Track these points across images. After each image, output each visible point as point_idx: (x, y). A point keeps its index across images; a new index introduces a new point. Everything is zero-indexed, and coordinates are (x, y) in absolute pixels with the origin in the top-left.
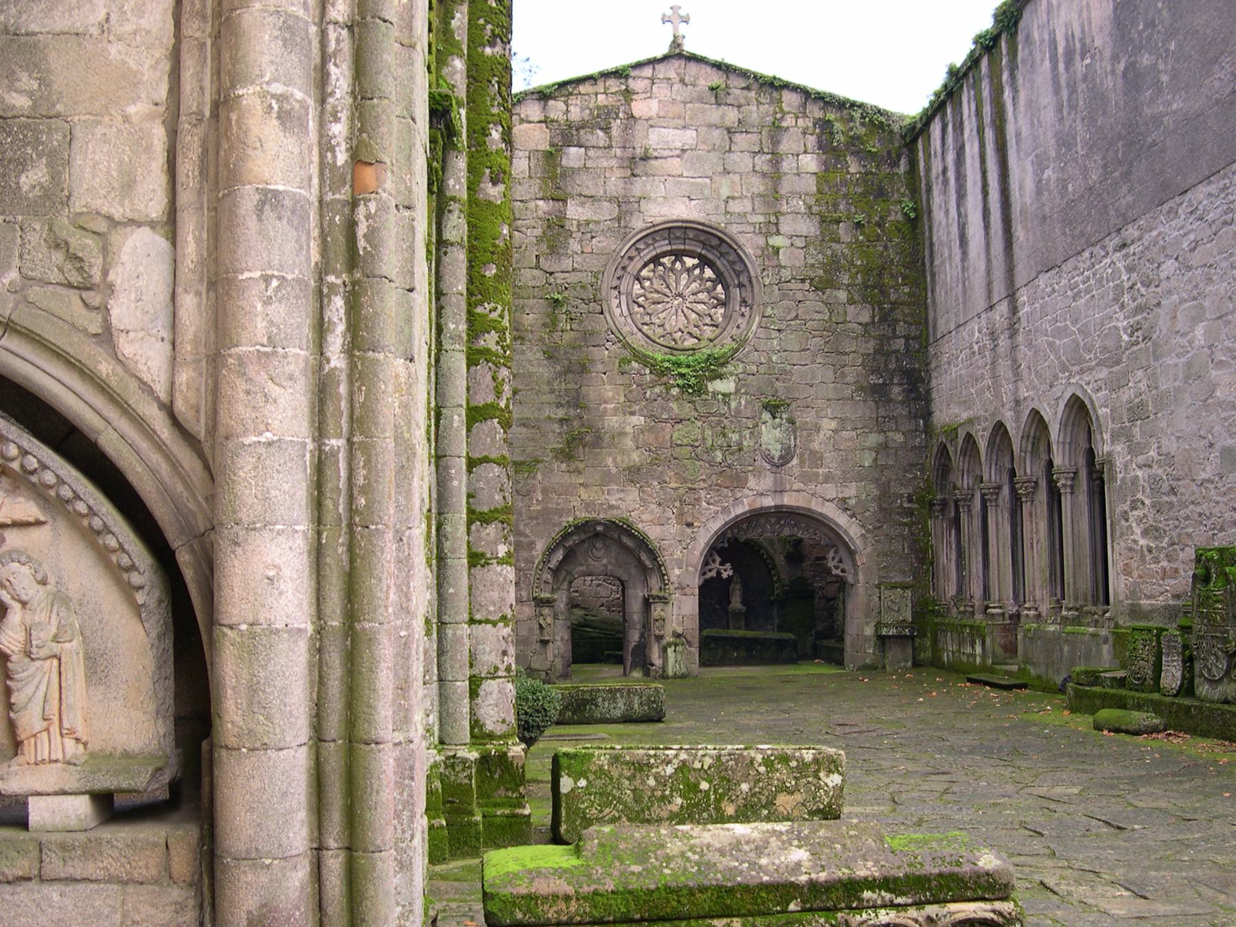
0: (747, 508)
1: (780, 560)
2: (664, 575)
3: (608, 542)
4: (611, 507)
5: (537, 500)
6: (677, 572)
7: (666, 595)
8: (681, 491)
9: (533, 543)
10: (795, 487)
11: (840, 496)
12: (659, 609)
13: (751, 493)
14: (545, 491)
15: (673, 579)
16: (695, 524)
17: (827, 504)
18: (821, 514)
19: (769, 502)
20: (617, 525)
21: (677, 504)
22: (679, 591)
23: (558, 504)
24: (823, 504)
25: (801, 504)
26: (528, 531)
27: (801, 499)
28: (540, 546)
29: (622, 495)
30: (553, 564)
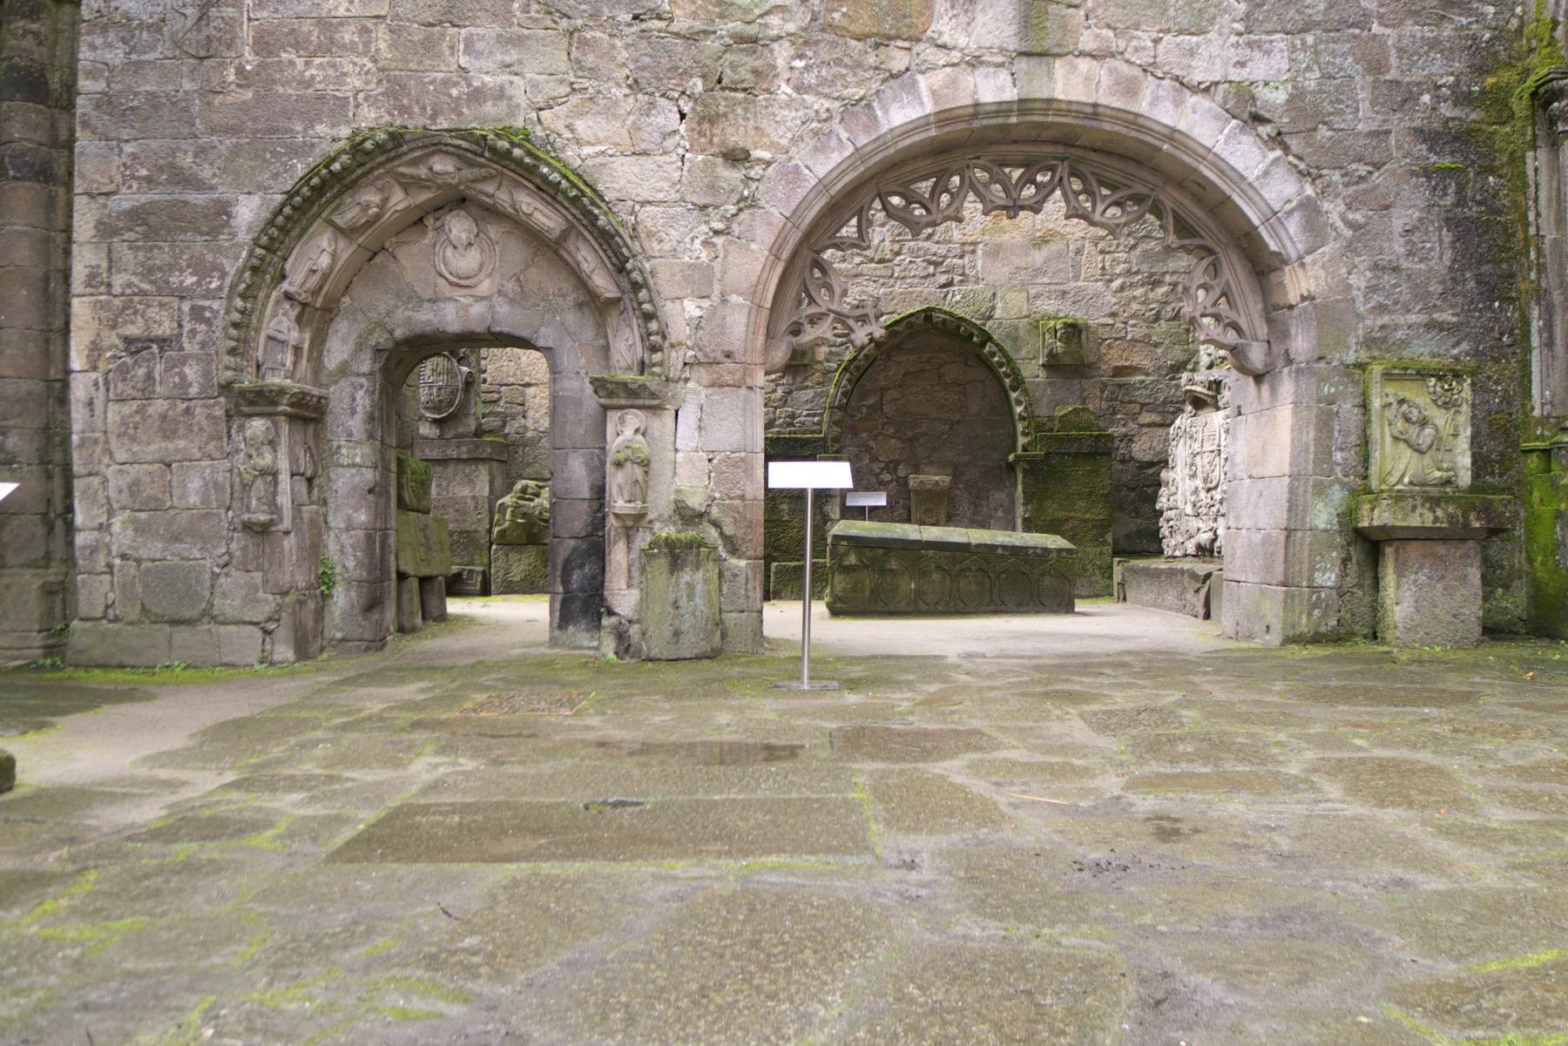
0: (929, 108)
1: (1032, 370)
2: (649, 317)
3: (494, 231)
4: (477, 95)
5: (240, 71)
6: (692, 308)
7: (652, 383)
8: (711, 45)
9: (223, 210)
10: (1087, 41)
11: (1235, 74)
12: (628, 432)
13: (941, 58)
14: (264, 45)
15: (679, 330)
16: (757, 153)
17: (1192, 100)
18: (1172, 135)
19: (993, 88)
20: (493, 149)
21: (697, 85)
22: (702, 374)
23: (309, 83)
24: (1178, 103)
25: (1108, 98)
26: (206, 173)
27: (1106, 80)
28: (248, 212)
29: (512, 56)
30: (297, 278)
